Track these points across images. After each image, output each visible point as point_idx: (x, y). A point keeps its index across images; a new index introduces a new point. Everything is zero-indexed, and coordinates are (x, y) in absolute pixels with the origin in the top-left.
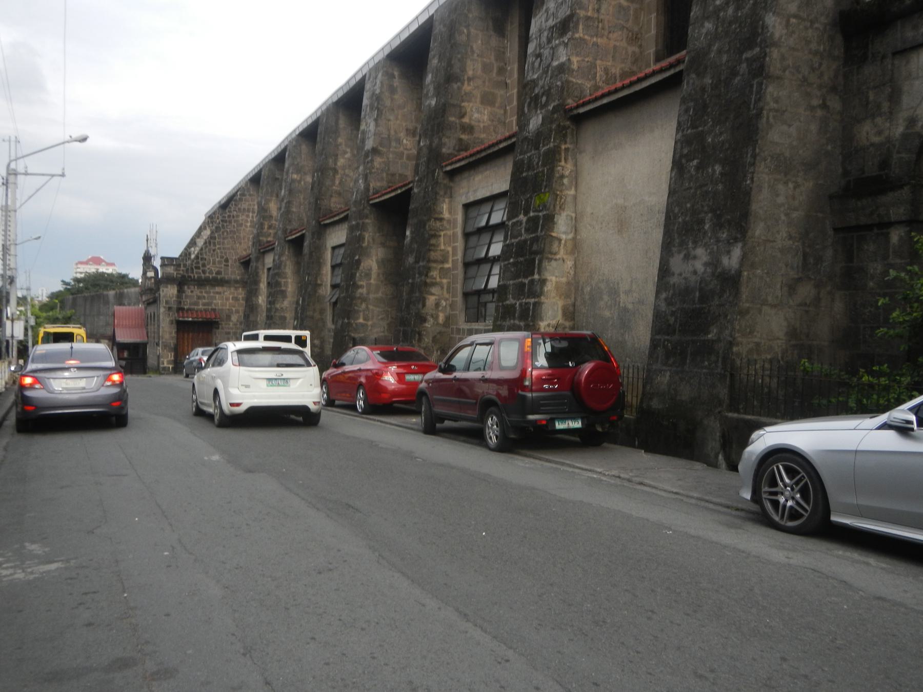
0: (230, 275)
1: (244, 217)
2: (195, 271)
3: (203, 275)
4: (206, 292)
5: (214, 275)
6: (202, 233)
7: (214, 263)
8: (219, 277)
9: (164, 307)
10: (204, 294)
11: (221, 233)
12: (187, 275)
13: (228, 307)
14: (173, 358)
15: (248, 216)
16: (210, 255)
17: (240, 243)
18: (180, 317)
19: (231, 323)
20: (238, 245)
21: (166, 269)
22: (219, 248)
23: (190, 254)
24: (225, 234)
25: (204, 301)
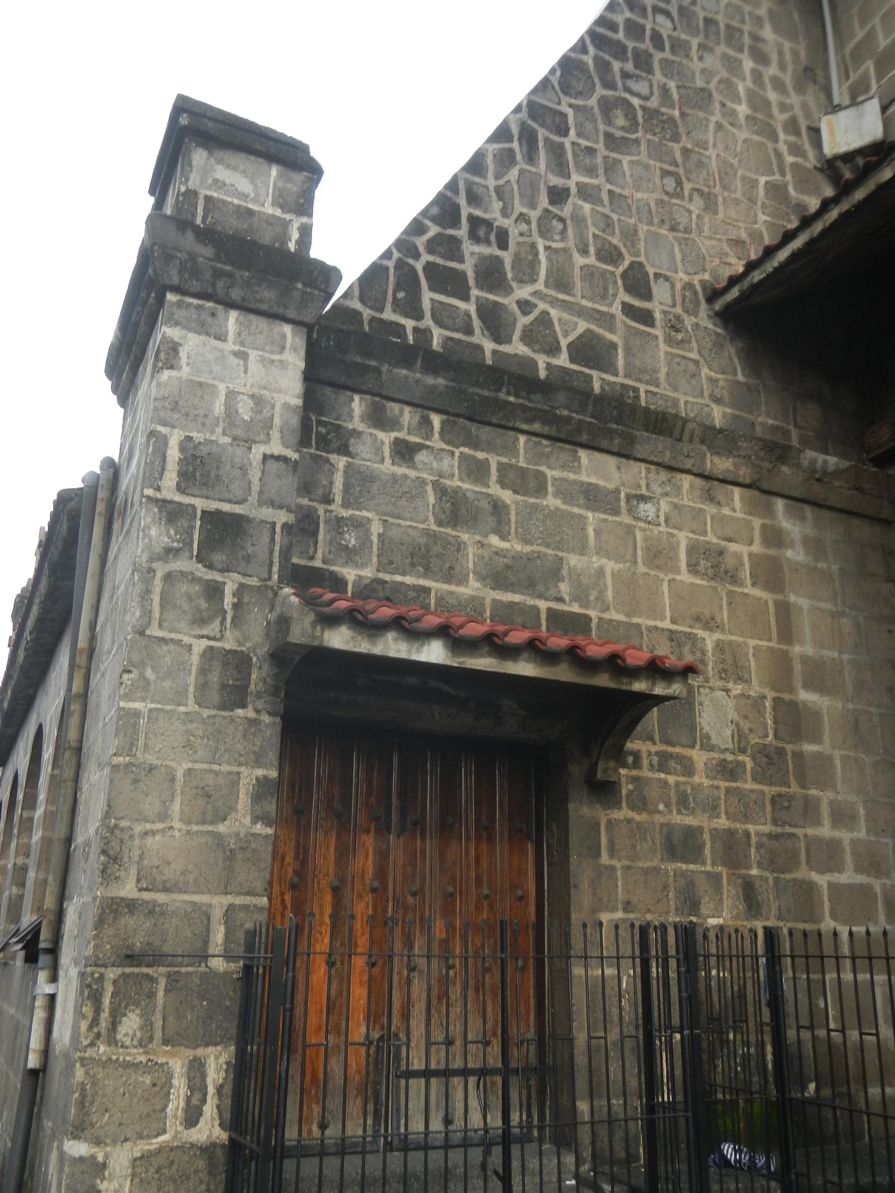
0: (664, 390)
1: (711, 61)
2: (428, 297)
3: (489, 346)
5: (563, 360)
8: (598, 380)
10: (495, 490)
11: (593, 102)
12: (368, 314)
13: (666, 624)
15: (733, 66)
16: (534, 215)
17: (710, 203)
18: (331, 621)
19: (699, 757)
20: (696, 206)
21: (222, 173)
22: (585, 192)
24: (621, 121)
25: (494, 540)
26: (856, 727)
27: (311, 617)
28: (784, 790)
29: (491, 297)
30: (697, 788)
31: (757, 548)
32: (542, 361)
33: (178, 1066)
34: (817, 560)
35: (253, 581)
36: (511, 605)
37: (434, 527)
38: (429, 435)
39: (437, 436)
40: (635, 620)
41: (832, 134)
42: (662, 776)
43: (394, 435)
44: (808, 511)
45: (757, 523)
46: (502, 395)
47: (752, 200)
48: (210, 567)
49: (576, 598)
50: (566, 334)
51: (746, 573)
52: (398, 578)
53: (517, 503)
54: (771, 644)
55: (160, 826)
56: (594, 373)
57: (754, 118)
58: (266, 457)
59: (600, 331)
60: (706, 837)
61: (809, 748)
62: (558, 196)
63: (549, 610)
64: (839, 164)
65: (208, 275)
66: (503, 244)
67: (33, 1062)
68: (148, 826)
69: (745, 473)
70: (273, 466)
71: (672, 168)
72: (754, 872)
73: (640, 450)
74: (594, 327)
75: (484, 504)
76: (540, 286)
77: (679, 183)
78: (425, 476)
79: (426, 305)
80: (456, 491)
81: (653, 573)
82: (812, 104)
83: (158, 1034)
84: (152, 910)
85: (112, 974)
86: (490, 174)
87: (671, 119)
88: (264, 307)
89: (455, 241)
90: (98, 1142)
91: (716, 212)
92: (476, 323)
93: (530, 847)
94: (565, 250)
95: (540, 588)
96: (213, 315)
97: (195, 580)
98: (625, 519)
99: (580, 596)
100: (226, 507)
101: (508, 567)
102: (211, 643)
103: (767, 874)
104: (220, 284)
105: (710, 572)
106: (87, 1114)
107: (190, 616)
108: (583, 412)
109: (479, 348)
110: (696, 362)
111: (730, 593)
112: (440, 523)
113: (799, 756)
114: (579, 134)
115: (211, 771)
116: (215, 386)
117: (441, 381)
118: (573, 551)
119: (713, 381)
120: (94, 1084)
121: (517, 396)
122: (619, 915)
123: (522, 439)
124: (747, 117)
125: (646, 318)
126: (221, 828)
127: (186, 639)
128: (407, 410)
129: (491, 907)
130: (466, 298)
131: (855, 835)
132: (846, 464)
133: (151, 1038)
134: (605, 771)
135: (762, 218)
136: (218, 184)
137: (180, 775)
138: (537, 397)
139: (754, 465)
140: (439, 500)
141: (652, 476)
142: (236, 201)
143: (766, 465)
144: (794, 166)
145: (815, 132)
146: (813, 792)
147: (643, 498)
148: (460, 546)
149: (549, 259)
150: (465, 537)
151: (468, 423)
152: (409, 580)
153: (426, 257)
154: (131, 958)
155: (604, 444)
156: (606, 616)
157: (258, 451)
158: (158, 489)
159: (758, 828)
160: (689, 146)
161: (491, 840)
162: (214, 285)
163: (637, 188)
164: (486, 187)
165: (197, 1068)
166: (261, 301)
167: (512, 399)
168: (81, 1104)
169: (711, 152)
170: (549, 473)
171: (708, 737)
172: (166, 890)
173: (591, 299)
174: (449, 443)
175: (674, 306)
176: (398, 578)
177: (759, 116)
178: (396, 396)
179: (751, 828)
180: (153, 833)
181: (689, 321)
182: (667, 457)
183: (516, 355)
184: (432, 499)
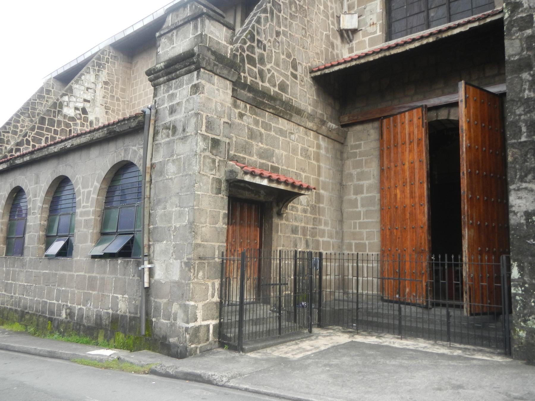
0: (298, 100)
3: (260, 83)
4: (267, 127)
5: (277, 89)
6: (83, 77)
7: (277, 65)
9: (205, 138)
13: (295, 170)
14: (216, 299)
16: (272, 40)
18: (246, 173)
19: (300, 207)
20: (309, 40)
21: (212, 28)
23: (61, 105)
24: (293, 9)
25: (260, 144)
26: (331, 200)
27: (243, 172)
28: (315, 216)
29: (262, 67)
30: (299, 215)
31: (315, 149)
32: (272, 89)
33: (210, 284)
34: (327, 153)
35: (222, 159)
36: (263, 163)
37: (247, 140)
38: (246, 112)
39: (248, 111)
40: (289, 169)
41: (343, 21)
42: (292, 212)
43: (239, 110)
44: (326, 139)
45: (315, 142)
46: (264, 101)
47: (322, 40)
48: (213, 154)
49: (277, 162)
50: (278, 81)
51: (312, 157)
52: (239, 154)
53: (265, 133)
54: (316, 177)
55: (205, 225)
56: (283, 94)
57: (324, 11)
58: (224, 122)
59: (285, 80)
60: (300, 228)
61: (321, 205)
62: (278, 34)
63: (271, 165)
64: (344, 32)
65: (212, 65)
66: (265, 50)
67: (146, 285)
68: (203, 225)
69: (315, 128)
70: (226, 125)
71: (304, 27)
72: (308, 237)
73: (293, 119)
74: (284, 79)
75: (258, 133)
76: (272, 64)
77: (306, 32)
78: (245, 124)
79: (246, 69)
80: (252, 129)
81: (293, 155)
82: (338, 7)
83: (206, 277)
84: (204, 247)
85: (197, 262)
86: (262, 25)
87: (305, 10)
88: (224, 76)
89: (253, 47)
90: (196, 302)
91: (313, 43)
92: (258, 76)
93: (258, 229)
94: (279, 53)
95: (269, 159)
96: (212, 77)
97: (210, 158)
98: (288, 139)
99: (277, 162)
100: (216, 137)
101: (263, 152)
102: (214, 176)
103: (311, 238)
104: (215, 68)
105: (305, 156)
106: (193, 295)
107: (209, 168)
108: (282, 107)
109: (258, 83)
110: (306, 92)
111: (309, 162)
112: (248, 139)
113: (319, 207)
114: (284, 13)
115: (214, 211)
116: (212, 100)
117: (251, 95)
118: (276, 148)
119: (309, 98)
120: (194, 288)
121: (268, 101)
122: (281, 248)
123: (267, 113)
124: (323, 10)
125: (295, 76)
126: (217, 226)
127: (209, 175)
128: (242, 102)
129: (250, 245)
130: (255, 67)
131: (328, 228)
132: (337, 127)
133: (205, 278)
134: (283, 211)
135: (324, 46)
136: (212, 32)
137: (208, 211)
138: (272, 102)
139: (317, 126)
140: (248, 131)
141: (294, 127)
142: (216, 39)
143: (320, 126)
144: (332, 28)
145: (338, 18)
146: (321, 217)
147: (292, 133)
148: (252, 146)
149: (275, 55)
150: (254, 143)
151: (255, 108)
152: (241, 155)
153: (247, 52)
154: (200, 258)
155: (285, 117)
156: (283, 167)
157: (223, 120)
158: (201, 131)
159: (310, 226)
160: (309, 20)
161: (250, 227)
162: (213, 68)
163: (296, 33)
164: (261, 29)
165: (213, 284)
166: (223, 74)
167: (267, 102)
168: (192, 293)
169: (314, 22)
170: (273, 125)
171: (301, 202)
172: (206, 241)
173: (284, 70)
174: (251, 114)
175: (302, 74)
176: (239, 154)
177: (325, 11)
178: (240, 99)
179: (308, 226)
180: (203, 227)
181: (305, 79)
182: (298, 122)
183: (266, 87)
184: (247, 131)
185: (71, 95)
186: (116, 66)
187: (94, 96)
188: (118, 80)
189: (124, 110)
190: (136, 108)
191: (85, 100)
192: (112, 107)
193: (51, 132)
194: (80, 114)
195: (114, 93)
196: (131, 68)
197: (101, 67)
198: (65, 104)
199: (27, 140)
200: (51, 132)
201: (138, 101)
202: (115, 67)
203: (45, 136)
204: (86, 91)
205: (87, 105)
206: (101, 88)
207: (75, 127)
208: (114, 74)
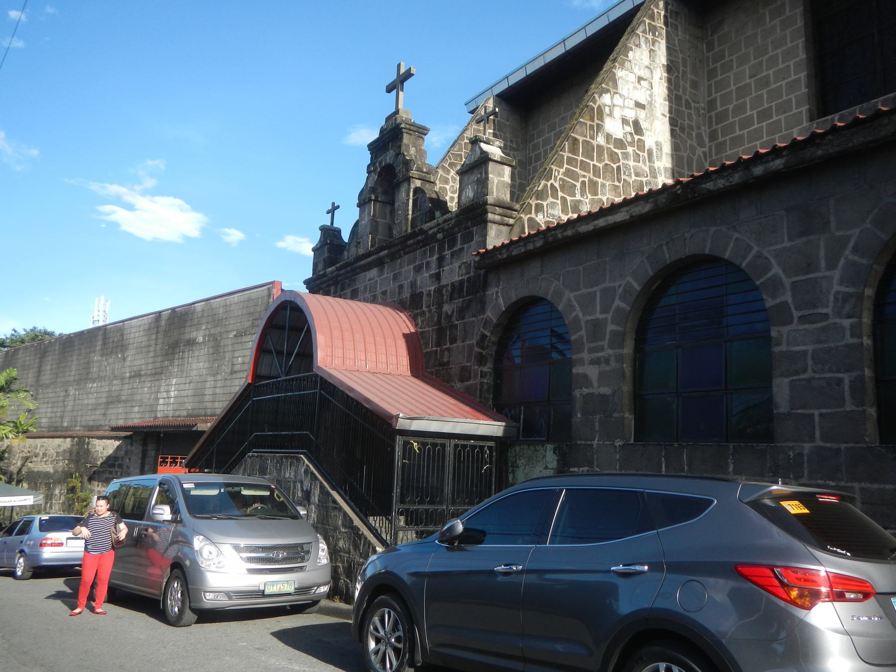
185: (615, 93)
186: (680, 33)
187: (651, 96)
188: (685, 66)
189: (699, 128)
190: (731, 120)
191: (639, 105)
192: (680, 121)
193: (589, 172)
194: (631, 134)
195: (681, 91)
196: (703, 39)
197: (657, 34)
198: (607, 110)
199: (552, 185)
200: (589, 172)
201: (735, 103)
202: (677, 35)
203: (581, 179)
204: (638, 86)
205: (642, 115)
206: (660, 79)
207: (626, 162)
208: (678, 49)
